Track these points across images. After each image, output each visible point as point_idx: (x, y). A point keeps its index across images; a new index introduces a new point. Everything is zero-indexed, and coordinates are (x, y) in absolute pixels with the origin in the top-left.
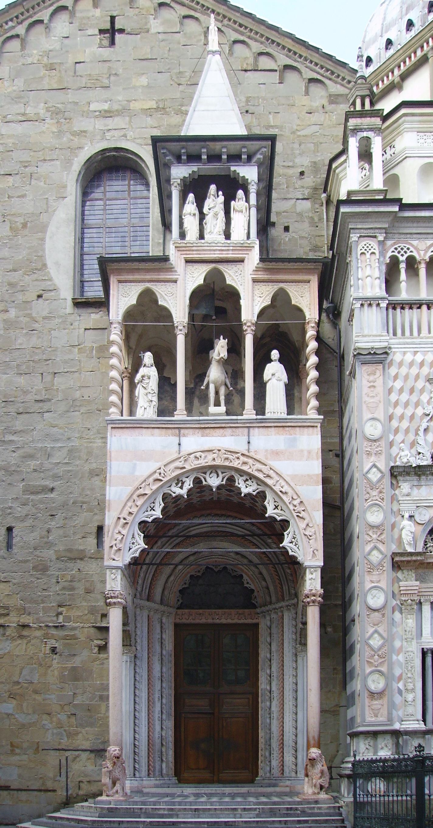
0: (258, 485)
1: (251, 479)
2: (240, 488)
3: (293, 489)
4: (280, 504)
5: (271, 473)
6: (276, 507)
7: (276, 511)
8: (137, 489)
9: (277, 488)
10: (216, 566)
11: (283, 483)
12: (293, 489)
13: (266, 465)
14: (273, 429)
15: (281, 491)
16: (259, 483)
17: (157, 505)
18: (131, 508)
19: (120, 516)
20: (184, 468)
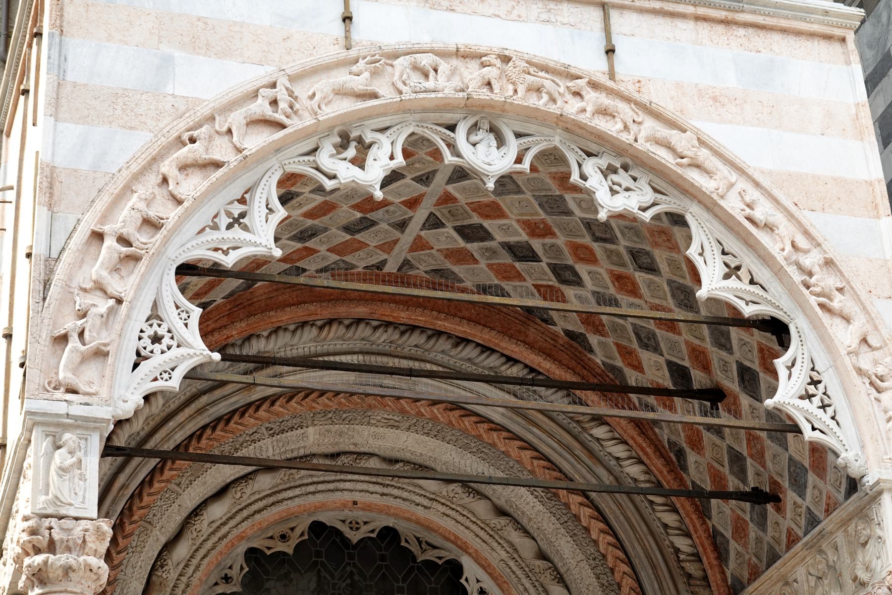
0: (656, 190)
1: (626, 168)
2: (590, 193)
3: (791, 216)
4: (748, 261)
5: (703, 154)
6: (733, 271)
7: (733, 282)
8: (180, 142)
9: (733, 205)
10: (355, 526)
11: (753, 194)
12: (791, 216)
13: (684, 131)
14: (691, 24)
15: (749, 219)
16: (661, 185)
17: (257, 210)
18: (149, 202)
19: (106, 228)
20: (374, 96)
